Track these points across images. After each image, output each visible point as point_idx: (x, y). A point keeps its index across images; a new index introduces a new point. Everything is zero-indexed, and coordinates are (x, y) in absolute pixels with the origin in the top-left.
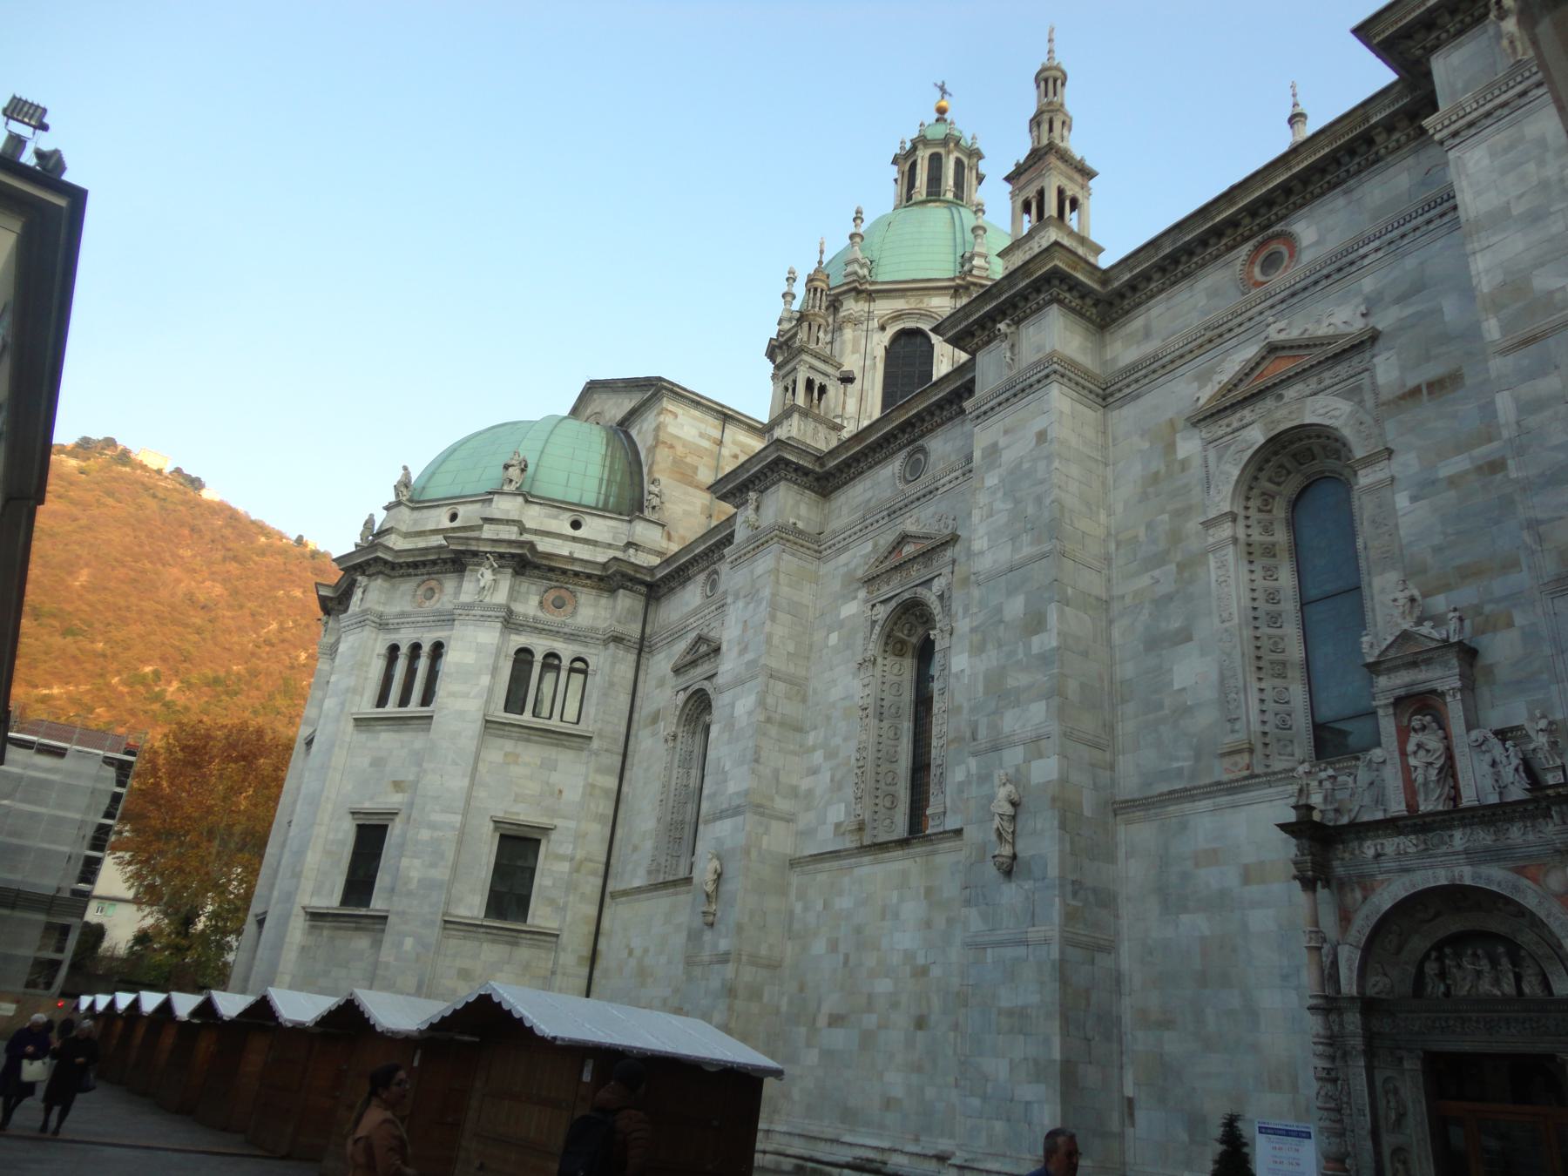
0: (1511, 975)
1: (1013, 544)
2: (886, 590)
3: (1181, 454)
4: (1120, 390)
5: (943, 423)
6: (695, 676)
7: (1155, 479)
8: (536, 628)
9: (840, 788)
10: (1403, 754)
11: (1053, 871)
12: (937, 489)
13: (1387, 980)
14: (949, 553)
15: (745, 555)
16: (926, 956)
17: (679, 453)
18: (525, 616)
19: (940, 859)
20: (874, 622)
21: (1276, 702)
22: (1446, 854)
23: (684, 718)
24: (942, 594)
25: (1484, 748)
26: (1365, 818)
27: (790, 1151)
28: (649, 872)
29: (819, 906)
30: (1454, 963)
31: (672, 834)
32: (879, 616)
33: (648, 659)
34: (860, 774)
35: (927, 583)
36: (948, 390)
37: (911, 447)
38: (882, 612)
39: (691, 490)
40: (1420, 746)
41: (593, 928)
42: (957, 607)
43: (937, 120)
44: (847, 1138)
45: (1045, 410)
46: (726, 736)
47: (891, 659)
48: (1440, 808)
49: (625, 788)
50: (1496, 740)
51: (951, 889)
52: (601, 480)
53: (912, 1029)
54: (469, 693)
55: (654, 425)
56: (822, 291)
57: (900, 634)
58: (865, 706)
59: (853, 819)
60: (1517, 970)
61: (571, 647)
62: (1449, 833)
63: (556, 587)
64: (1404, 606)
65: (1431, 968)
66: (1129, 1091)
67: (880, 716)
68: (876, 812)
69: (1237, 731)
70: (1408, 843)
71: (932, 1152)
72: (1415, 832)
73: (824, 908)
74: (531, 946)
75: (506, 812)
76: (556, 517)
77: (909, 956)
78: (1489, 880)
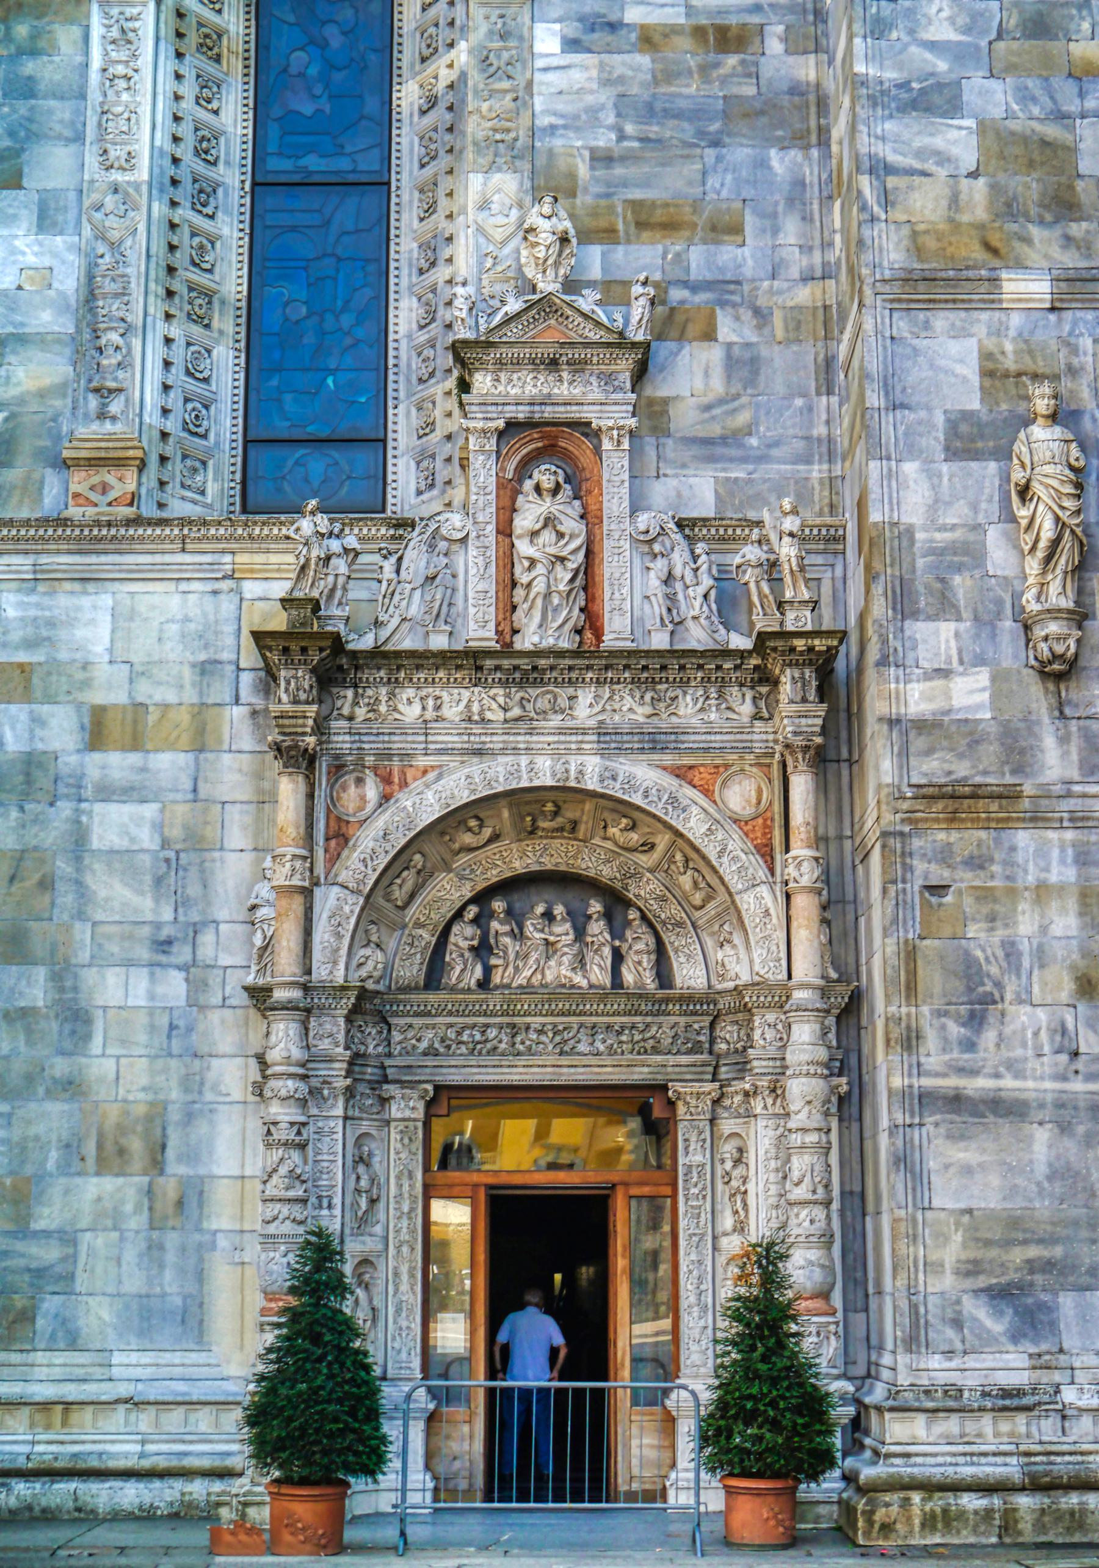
0: (607, 951)
10: (505, 530)
13: (380, 956)
21: (188, 373)
22: (561, 731)
25: (657, 547)
26: (408, 643)
30: (507, 928)
40: (549, 521)
48: (565, 644)
50: (678, 537)
60: (617, 943)
62: (571, 691)
64: (548, 247)
65: (463, 936)
69: (114, 418)
72: (505, 684)
78: (630, 784)
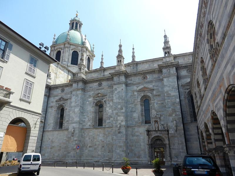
3: (135, 94)
7: (132, 95)
11: (124, 133)
19: (105, 130)
20: (94, 102)
28: (53, 129)
29: (87, 134)
35: (103, 99)
38: (95, 101)
41: (42, 136)
42: (107, 103)
46: (73, 113)
65: (155, 141)
66: (129, 152)
67: (95, 113)
70: (155, 132)
77: (101, 140)
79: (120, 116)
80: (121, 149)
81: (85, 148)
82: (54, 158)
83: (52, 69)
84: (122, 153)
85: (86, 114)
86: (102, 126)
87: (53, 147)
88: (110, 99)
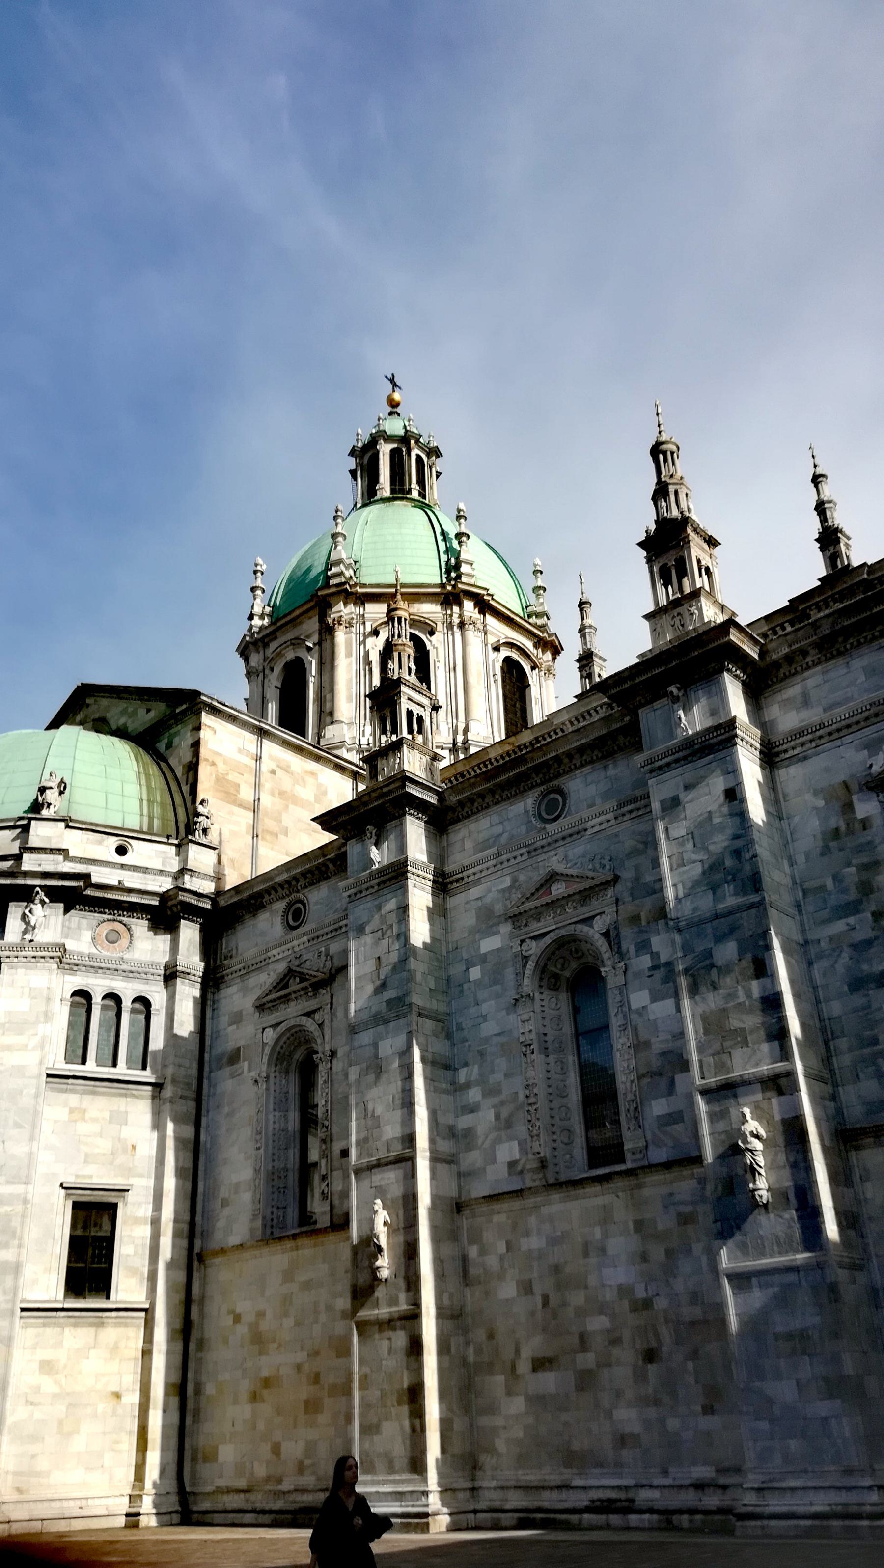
1: (714, 893)
2: (537, 927)
4: (786, 751)
5: (582, 766)
6: (291, 1012)
7: (836, 834)
8: (93, 967)
9: (509, 1124)
12: (586, 830)
14: (610, 892)
15: (367, 889)
16: (646, 1290)
17: (220, 771)
18: (81, 954)
19: (646, 1192)
23: (275, 1057)
24: (608, 931)
27: (508, 1506)
29: (502, 1248)
31: (274, 1183)
32: (530, 952)
33: (214, 994)
34: (533, 1111)
36: (592, 737)
37: (545, 787)
38: (534, 949)
39: (236, 809)
42: (628, 945)
43: (391, 414)
44: (578, 1482)
45: (730, 770)
47: (547, 994)
49: (203, 1137)
51: (665, 1222)
52: (141, 800)
53: (640, 1362)
54: (26, 1046)
55: (190, 741)
56: (405, 620)
57: (553, 969)
58: (527, 1043)
59: (531, 1156)
61: (130, 985)
63: (109, 920)
67: (545, 1051)
68: (555, 1149)
71: (687, 1482)
73: (508, 1251)
74: (117, 1325)
75: (77, 1176)
76: (100, 843)
77: (624, 1291)
79: (745, 1043)
80: (807, 1369)
81: (500, 1379)
82: (279, 1481)
83: (221, 780)
84: (823, 1408)
85: (476, 1069)
86: (623, 1161)
87: (267, 1383)
88: (647, 906)
